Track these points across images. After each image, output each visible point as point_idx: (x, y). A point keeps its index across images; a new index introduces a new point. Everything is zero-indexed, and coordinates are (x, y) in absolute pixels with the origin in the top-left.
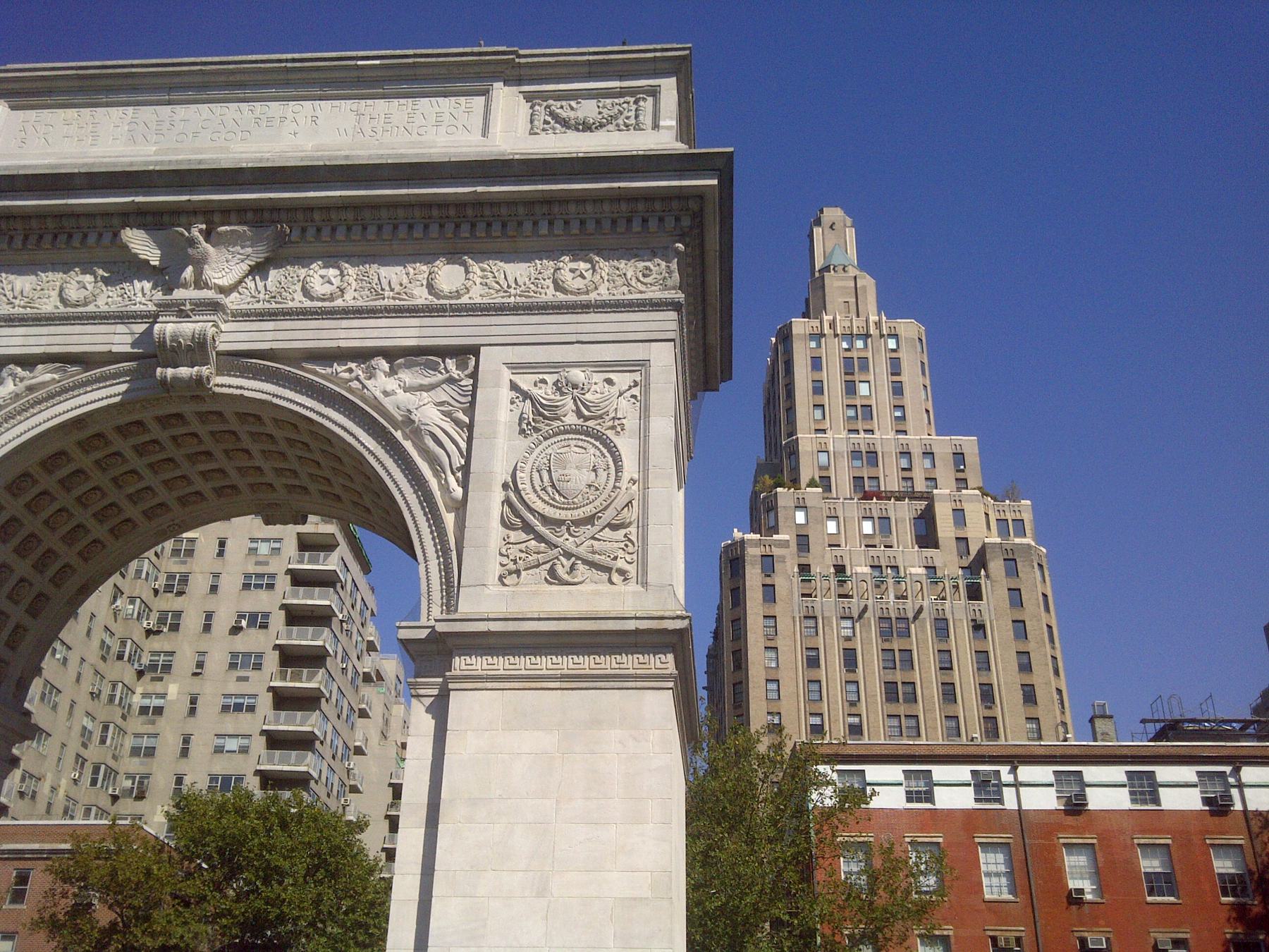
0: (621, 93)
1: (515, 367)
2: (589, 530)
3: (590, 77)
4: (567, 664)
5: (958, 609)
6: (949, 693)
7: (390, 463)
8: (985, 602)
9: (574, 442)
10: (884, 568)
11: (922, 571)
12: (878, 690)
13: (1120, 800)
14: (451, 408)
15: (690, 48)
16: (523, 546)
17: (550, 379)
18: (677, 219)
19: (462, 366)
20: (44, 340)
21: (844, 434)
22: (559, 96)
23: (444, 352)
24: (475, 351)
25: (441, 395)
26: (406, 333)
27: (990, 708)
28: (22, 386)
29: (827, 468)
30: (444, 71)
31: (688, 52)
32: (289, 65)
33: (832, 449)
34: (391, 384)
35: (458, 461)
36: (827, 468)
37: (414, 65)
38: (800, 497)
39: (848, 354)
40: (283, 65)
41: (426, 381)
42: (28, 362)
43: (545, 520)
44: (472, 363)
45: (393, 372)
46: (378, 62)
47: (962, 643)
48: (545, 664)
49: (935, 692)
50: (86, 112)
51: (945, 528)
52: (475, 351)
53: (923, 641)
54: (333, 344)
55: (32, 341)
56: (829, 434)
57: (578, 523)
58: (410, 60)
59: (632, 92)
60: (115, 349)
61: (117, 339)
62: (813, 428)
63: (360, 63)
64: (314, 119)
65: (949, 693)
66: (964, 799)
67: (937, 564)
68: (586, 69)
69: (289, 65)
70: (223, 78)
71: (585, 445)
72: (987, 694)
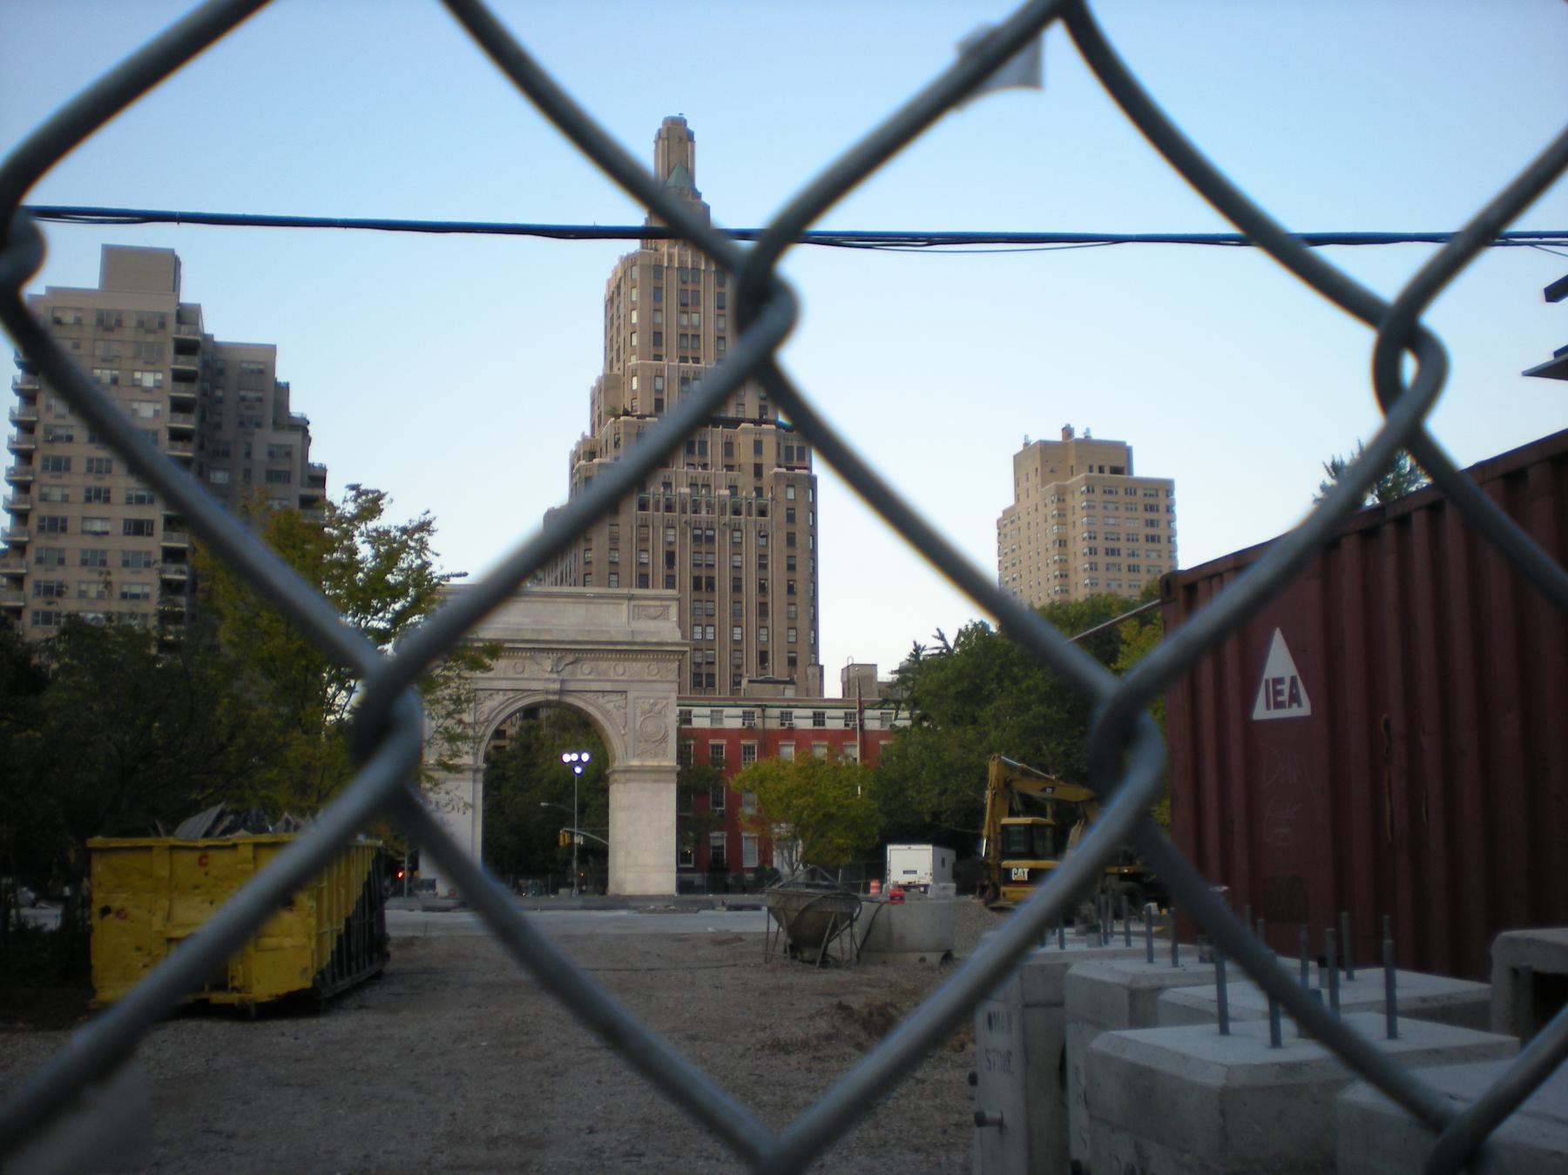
0: (662, 606)
1: (637, 698)
5: (748, 521)
6: (737, 587)
8: (769, 518)
10: (700, 486)
11: (727, 492)
12: (688, 583)
13: (807, 724)
21: (676, 363)
22: (642, 606)
24: (626, 692)
26: (608, 686)
27: (764, 596)
28: (506, 698)
29: (661, 392)
33: (666, 375)
35: (623, 724)
36: (661, 392)
38: (641, 425)
39: (684, 287)
45: (603, 697)
47: (751, 543)
49: (728, 584)
51: (745, 456)
52: (626, 692)
53: (724, 541)
56: (665, 362)
62: (653, 352)
65: (737, 587)
66: (737, 724)
67: (740, 485)
72: (762, 588)
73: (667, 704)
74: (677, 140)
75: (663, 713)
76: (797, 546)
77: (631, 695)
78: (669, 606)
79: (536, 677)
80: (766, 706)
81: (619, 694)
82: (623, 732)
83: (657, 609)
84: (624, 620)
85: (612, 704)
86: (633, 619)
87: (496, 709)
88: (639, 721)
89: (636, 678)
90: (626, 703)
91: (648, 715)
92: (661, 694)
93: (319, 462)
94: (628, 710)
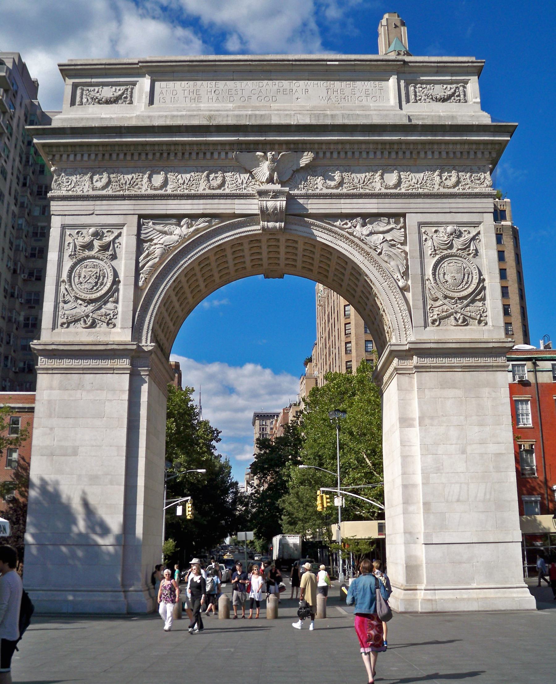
2: (465, 302)
3: (437, 73)
4: (465, 361)
7: (371, 267)
9: (455, 261)
14: (395, 243)
15: (484, 62)
16: (437, 309)
17: (441, 229)
18: (490, 153)
19: (397, 222)
20: (202, 207)
23: (389, 216)
24: (404, 215)
25: (388, 237)
30: (368, 68)
31: (483, 64)
32: (294, 63)
34: (366, 230)
37: (355, 65)
40: (291, 63)
41: (381, 229)
42: (194, 217)
43: (446, 297)
44: (402, 220)
45: (364, 225)
46: (337, 63)
48: (455, 361)
50: (191, 83)
52: (404, 215)
54: (339, 211)
55: (195, 207)
57: (460, 299)
58: (353, 63)
59: (457, 82)
60: (237, 212)
61: (236, 207)
63: (328, 63)
64: (307, 91)
68: (436, 69)
69: (294, 63)
70: (260, 68)
71: (460, 262)
73: (479, 233)
74: (394, 26)
75: (472, 248)
76: (508, 278)
77: (412, 220)
78: (466, 82)
79: (245, 192)
80: (537, 359)
81: (392, 220)
82: (401, 283)
83: (445, 86)
84: (393, 100)
85: (381, 236)
86: (408, 101)
87: (175, 248)
88: (430, 263)
89: (420, 191)
90: (405, 236)
91: (445, 252)
92: (466, 218)
93: (36, 77)
94: (407, 249)
